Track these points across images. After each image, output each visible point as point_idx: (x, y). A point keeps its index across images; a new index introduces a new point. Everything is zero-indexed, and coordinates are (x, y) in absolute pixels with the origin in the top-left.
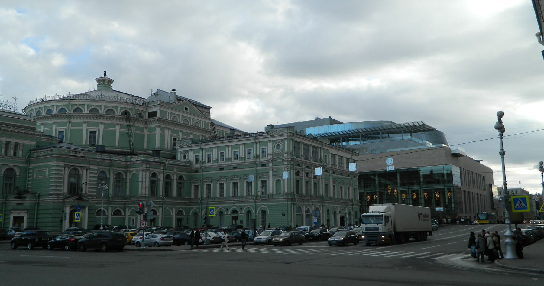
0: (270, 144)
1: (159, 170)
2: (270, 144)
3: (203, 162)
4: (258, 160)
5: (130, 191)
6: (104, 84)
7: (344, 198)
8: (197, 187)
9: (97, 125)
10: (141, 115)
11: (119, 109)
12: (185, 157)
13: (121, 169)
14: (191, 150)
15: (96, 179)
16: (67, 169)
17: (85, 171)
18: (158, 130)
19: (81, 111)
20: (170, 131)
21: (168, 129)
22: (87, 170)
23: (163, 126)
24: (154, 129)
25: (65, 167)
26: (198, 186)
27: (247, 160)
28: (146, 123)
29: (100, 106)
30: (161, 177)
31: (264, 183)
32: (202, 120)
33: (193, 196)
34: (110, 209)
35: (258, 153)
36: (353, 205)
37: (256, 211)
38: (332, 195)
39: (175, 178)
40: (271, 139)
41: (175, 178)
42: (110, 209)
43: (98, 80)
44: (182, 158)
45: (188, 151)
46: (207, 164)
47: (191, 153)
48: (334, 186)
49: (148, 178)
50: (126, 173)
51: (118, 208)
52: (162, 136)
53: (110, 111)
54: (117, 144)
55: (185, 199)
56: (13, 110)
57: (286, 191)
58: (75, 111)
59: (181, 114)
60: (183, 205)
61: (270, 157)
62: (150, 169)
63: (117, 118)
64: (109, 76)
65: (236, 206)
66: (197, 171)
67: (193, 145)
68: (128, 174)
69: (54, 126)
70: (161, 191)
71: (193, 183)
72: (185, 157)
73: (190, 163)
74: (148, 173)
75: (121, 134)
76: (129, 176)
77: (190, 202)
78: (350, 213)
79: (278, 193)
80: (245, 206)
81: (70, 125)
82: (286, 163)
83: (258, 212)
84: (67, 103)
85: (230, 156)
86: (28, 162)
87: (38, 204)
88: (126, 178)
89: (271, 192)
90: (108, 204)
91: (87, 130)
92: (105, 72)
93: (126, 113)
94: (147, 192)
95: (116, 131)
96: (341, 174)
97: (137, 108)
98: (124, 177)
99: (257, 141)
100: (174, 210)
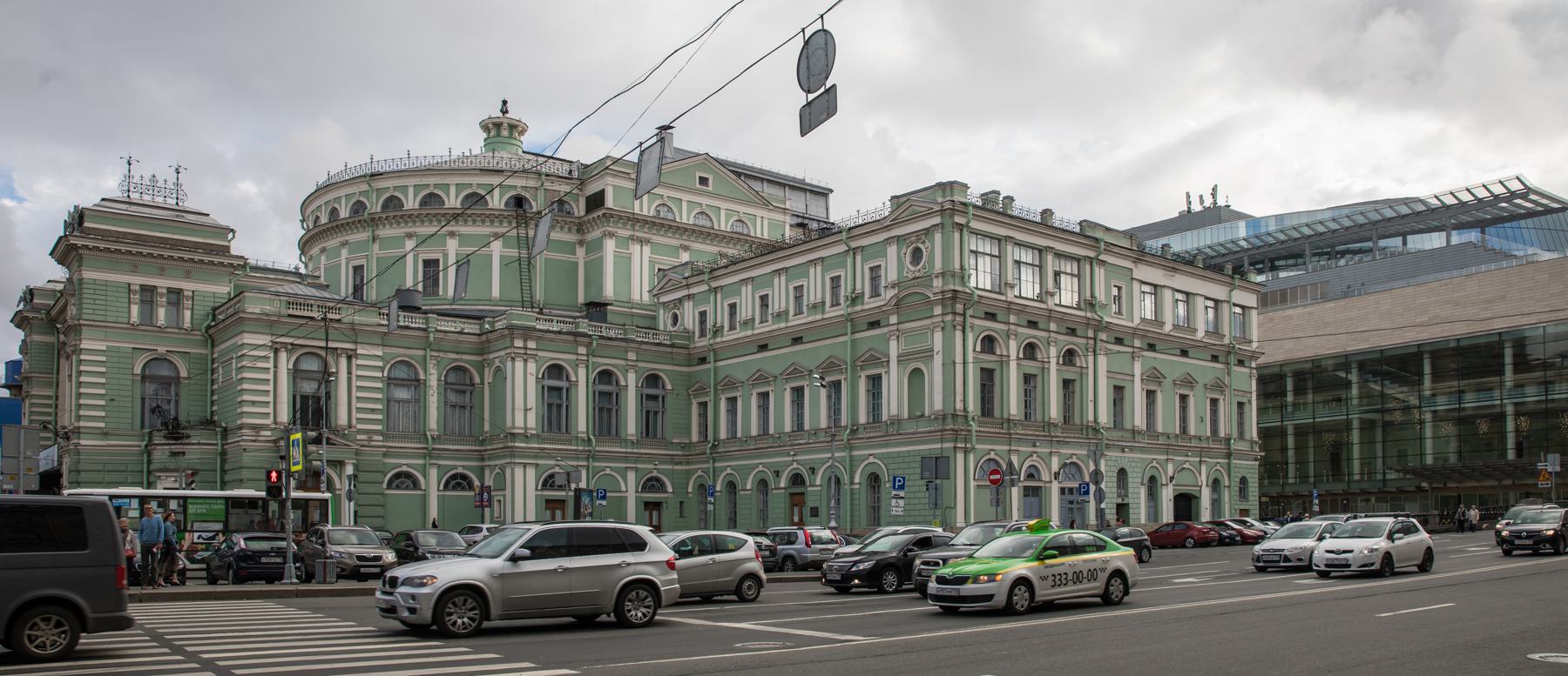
1: (573, 357)
3: (717, 331)
4: (859, 308)
5: (492, 424)
6: (498, 135)
7: (1192, 431)
8: (704, 405)
12: (675, 319)
13: (465, 357)
14: (689, 297)
15: (380, 385)
16: (283, 356)
17: (343, 362)
18: (610, 245)
20: (647, 249)
21: (641, 241)
22: (349, 358)
23: (624, 233)
25: (276, 351)
27: (831, 313)
28: (581, 228)
30: (582, 380)
31: (875, 381)
32: (760, 213)
33: (695, 437)
34: (433, 473)
35: (859, 286)
36: (1229, 456)
37: (852, 478)
38: (1139, 421)
39: (631, 383)
42: (433, 473)
43: (485, 127)
44: (669, 322)
46: (728, 336)
47: (688, 305)
48: (1150, 394)
49: (532, 381)
51: (460, 470)
52: (624, 262)
53: (475, 199)
54: (496, 293)
55: (669, 445)
56: (171, 202)
57: (938, 406)
59: (685, 197)
60: (662, 463)
61: (891, 293)
62: (540, 353)
63: (494, 217)
64: (513, 114)
65: (792, 463)
66: (703, 360)
67: (691, 281)
69: (344, 252)
70: (582, 421)
71: (696, 396)
72: (675, 319)
73: (688, 335)
74: (532, 366)
75: (506, 264)
76: (488, 379)
78: (1216, 485)
79: (917, 416)
81: (376, 246)
82: (938, 310)
83: (857, 480)
84: (365, 187)
85: (783, 305)
86: (211, 340)
87: (223, 454)
88: (482, 383)
89: (894, 411)
90: (424, 457)
92: (505, 102)
93: (519, 201)
94: (532, 423)
96: (1184, 353)
97: (547, 185)
98: (477, 380)
99: (854, 244)
100: (631, 476)
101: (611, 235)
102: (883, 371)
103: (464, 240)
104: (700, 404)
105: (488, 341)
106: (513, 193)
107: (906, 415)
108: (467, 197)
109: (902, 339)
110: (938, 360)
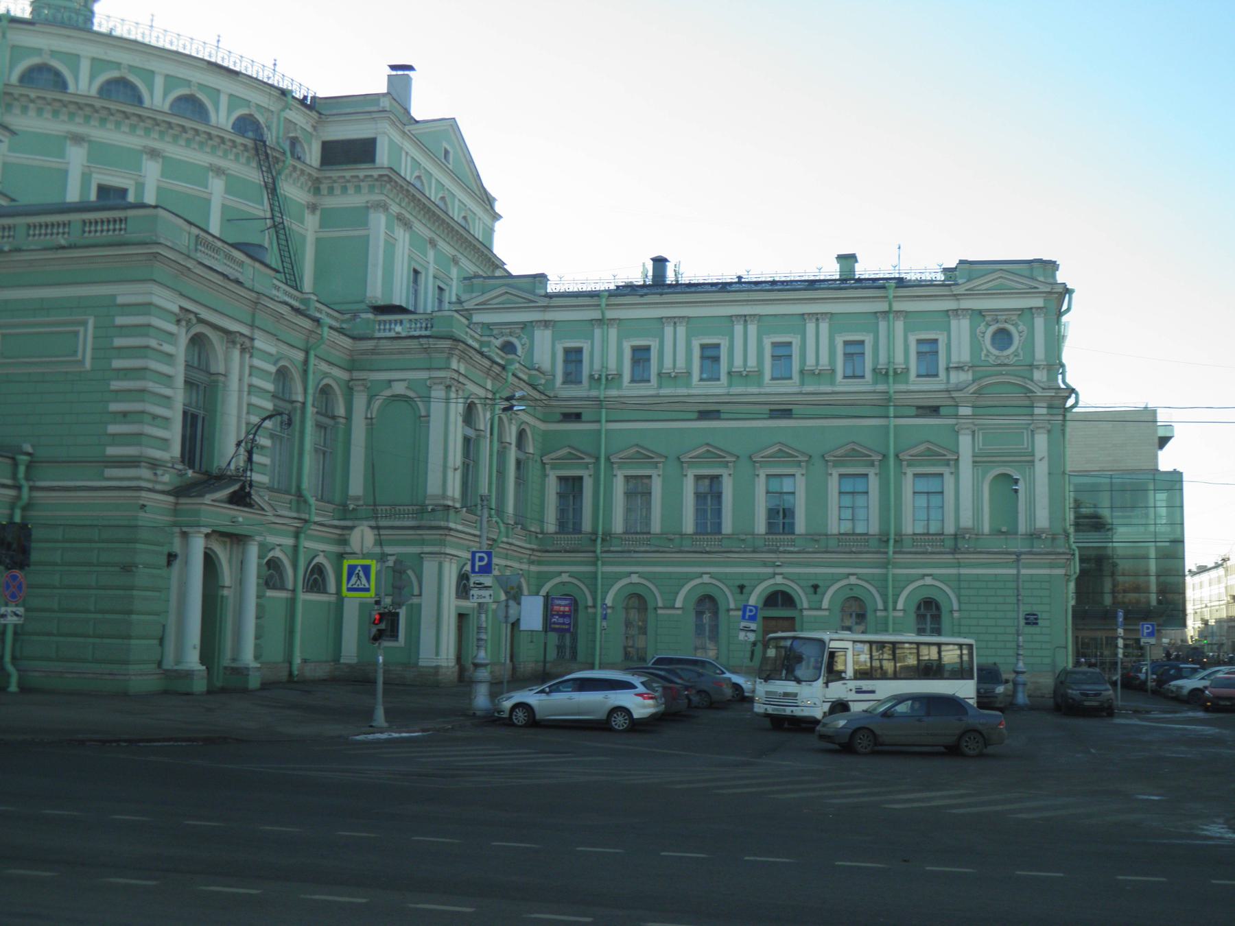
0: (961, 328)
2: (961, 328)
9: (131, 159)
10: (298, 149)
11: (224, 100)
14: (546, 324)
19: (61, 84)
23: (395, 209)
24: (360, 216)
26: (580, 479)
27: (843, 386)
28: (317, 191)
29: (149, 75)
37: (895, 603)
40: (966, 304)
41: (511, 436)
45: (524, 326)
46: (628, 389)
47: (543, 338)
50: (349, 390)
57: (1042, 520)
58: (29, 77)
63: (212, 140)
68: (360, 401)
71: (554, 467)
77: (598, 543)
80: (835, 579)
83: (900, 606)
85: (752, 362)
88: (348, 418)
91: (86, 178)
93: (246, 124)
95: (208, 201)
98: (341, 411)
101: (385, 207)
102: (946, 471)
103: (171, 168)
104: (561, 479)
105: (373, 352)
106: (245, 111)
107: (986, 529)
108: (180, 99)
109: (980, 437)
110: (1041, 469)
